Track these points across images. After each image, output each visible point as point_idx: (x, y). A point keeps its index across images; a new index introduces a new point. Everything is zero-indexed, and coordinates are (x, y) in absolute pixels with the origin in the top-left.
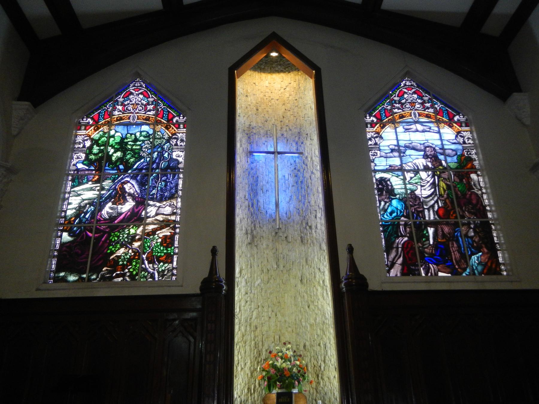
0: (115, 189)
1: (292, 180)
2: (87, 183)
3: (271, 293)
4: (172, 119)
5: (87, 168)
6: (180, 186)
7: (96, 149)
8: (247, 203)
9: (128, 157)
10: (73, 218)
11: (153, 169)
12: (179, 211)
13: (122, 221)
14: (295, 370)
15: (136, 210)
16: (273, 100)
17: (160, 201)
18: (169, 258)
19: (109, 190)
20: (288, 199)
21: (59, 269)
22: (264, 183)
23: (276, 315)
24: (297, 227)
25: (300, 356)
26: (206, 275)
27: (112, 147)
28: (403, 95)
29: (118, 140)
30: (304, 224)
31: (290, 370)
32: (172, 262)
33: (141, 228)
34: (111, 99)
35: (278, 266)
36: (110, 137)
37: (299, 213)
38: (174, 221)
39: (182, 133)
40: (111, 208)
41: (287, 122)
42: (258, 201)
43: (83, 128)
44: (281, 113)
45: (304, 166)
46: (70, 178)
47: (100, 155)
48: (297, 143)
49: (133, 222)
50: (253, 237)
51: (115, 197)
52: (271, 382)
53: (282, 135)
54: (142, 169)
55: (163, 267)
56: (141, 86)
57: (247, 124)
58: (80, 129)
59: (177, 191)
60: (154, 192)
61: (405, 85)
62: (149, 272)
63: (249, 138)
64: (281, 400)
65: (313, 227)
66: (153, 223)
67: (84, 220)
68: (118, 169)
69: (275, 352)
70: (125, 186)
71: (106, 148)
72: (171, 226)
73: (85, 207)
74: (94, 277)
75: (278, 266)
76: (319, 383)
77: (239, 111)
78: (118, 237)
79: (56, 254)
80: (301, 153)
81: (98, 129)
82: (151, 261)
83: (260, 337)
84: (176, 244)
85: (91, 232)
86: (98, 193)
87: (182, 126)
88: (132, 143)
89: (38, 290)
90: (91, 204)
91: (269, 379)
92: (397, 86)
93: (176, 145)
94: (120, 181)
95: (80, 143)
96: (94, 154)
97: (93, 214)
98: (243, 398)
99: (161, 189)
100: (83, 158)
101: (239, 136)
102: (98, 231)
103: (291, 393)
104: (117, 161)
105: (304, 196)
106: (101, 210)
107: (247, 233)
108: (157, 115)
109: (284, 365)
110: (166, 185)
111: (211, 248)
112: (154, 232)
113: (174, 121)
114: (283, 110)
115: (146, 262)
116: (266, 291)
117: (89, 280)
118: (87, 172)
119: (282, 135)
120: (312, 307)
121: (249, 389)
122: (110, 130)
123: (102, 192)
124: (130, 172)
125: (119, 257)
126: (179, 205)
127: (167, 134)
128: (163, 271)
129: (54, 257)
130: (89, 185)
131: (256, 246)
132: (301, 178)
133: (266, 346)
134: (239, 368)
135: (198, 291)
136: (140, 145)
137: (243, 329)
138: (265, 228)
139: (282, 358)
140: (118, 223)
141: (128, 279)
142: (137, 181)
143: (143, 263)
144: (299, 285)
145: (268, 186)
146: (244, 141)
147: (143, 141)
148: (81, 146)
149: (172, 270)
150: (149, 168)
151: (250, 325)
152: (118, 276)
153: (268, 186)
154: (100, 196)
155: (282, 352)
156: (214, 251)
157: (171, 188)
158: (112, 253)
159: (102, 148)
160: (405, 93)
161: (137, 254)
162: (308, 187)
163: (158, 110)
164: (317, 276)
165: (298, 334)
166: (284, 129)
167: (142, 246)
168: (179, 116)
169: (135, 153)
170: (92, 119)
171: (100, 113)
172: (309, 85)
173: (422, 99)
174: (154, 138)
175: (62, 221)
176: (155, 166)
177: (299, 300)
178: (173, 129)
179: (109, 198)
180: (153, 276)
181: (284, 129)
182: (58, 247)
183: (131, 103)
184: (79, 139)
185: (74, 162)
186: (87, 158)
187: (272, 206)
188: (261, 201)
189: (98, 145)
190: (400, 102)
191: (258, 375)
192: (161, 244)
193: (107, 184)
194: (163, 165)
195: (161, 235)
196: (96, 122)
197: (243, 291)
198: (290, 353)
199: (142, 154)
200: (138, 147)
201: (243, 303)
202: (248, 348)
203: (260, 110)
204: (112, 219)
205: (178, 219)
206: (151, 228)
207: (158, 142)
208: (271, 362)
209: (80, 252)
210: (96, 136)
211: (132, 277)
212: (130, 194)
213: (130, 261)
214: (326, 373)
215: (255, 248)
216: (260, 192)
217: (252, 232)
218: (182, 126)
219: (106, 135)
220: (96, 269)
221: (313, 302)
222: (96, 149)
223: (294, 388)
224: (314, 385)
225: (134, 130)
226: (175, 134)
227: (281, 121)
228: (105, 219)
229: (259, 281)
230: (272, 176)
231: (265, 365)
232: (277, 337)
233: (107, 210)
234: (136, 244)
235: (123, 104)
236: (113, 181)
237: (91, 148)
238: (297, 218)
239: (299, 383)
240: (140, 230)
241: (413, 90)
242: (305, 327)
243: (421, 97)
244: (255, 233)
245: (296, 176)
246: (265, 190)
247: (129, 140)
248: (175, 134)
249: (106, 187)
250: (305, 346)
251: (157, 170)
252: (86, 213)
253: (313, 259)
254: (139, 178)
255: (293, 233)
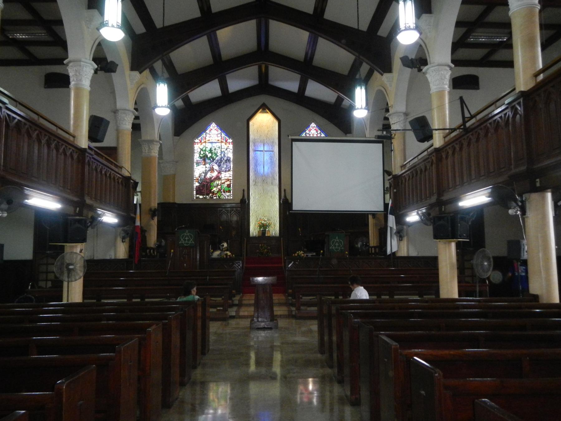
0: (210, 168)
1: (269, 161)
2: (201, 165)
3: (261, 201)
4: (227, 141)
5: (200, 160)
6: (232, 167)
7: (202, 153)
8: (253, 170)
9: (213, 156)
10: (198, 178)
11: (222, 160)
12: (232, 176)
13: (214, 179)
14: (267, 224)
15: (218, 175)
16: (263, 127)
17: (225, 172)
18: (229, 191)
19: (208, 168)
20: (268, 168)
21: (197, 194)
22: (260, 162)
23: (263, 208)
24: (270, 179)
25: (270, 220)
26: (241, 197)
27: (208, 152)
28: (310, 130)
29: (209, 149)
30: (273, 178)
31: (266, 224)
32: (231, 192)
33: (220, 181)
34: (205, 130)
35: (264, 192)
36: (206, 148)
37: (271, 174)
38: (230, 179)
39: (231, 146)
40: (210, 175)
41: (269, 136)
42: (257, 169)
43: (196, 144)
44: (266, 132)
45: (274, 156)
46: (195, 163)
47: (204, 155)
48: (272, 146)
49: (218, 179)
50: (256, 182)
51: (210, 170)
52: (260, 227)
53: (267, 142)
54: (218, 160)
55: (228, 194)
56: (215, 126)
57: (254, 138)
58: (195, 144)
59: (230, 169)
60: (223, 169)
61: (312, 126)
62: (224, 196)
63: (254, 144)
64: (263, 232)
65: (276, 179)
66: (224, 180)
67: (202, 178)
68: (210, 160)
69: (262, 219)
70: (213, 166)
71: (205, 152)
72: (230, 180)
73: (201, 174)
74: (207, 197)
75: (264, 192)
76: (275, 228)
77: (251, 133)
78: (213, 184)
79: (195, 189)
80: (273, 151)
81: (202, 144)
82: (224, 192)
83: (257, 215)
84: (231, 187)
85: (204, 182)
86: (205, 169)
87: (231, 143)
88: (214, 150)
89: (192, 201)
90: (203, 173)
91: (260, 226)
92: (309, 126)
93: (229, 151)
94: (212, 165)
95: (196, 150)
96: (202, 155)
97: (205, 176)
98: (252, 231)
99: (225, 168)
100: (199, 156)
101: (251, 144)
102: (207, 182)
103: (265, 230)
104: (210, 157)
105: (273, 168)
106: (206, 175)
107: (253, 181)
108: (221, 139)
109: (264, 223)
110: (227, 166)
111: (243, 189)
112: (224, 183)
113: (228, 141)
114: (267, 130)
115: (223, 192)
116: (260, 200)
117: (206, 198)
118: (200, 161)
119: (267, 142)
120: (274, 206)
121: (254, 229)
122: (206, 144)
123: (207, 169)
124: (214, 161)
125: (214, 191)
126: (232, 174)
127: (226, 147)
128: (228, 195)
129: (194, 190)
130: (202, 166)
131: (257, 185)
132: (273, 161)
133: (259, 217)
134: (251, 223)
135: (239, 202)
136: (217, 151)
137: (252, 212)
138: (260, 179)
139: (264, 221)
140: (213, 179)
141: (218, 198)
142: (217, 165)
143: (222, 193)
144: (270, 199)
145: (261, 163)
146: (252, 146)
147: (218, 150)
148: (197, 151)
149: (231, 195)
150: (221, 160)
151: (255, 211)
152: (215, 197)
153: (261, 163)
154: (206, 170)
155: (263, 219)
156: (244, 190)
157: (229, 168)
158: (212, 189)
159: (204, 152)
160: (311, 130)
161: (220, 190)
162: (275, 164)
163: (222, 137)
164: (276, 196)
165: (269, 214)
166: (267, 140)
167: (221, 187)
168: (229, 139)
169: (215, 154)
170: (199, 140)
171: (201, 138)
172: (276, 123)
173: (317, 132)
174: (221, 148)
175: (195, 178)
176: (222, 159)
177: (270, 203)
178: (228, 145)
179: (209, 170)
180: (225, 197)
181: (267, 140)
182: (195, 187)
183: (212, 134)
184: (195, 148)
185: (195, 157)
186: (200, 156)
187: (262, 171)
188: (258, 169)
189: (203, 151)
190: (309, 134)
191: (257, 225)
192: (227, 187)
193: (208, 165)
194: (225, 159)
195: (227, 184)
196: (201, 142)
197: (252, 201)
198: (266, 219)
199: (218, 154)
200: (216, 152)
201: (252, 204)
202: (254, 218)
203: (259, 131)
204: (211, 178)
205: (231, 178)
206: (223, 181)
207: (222, 150)
208: (260, 222)
209: (202, 189)
210: (201, 147)
211: (219, 197)
212: (215, 170)
213: (218, 192)
214: (277, 225)
215: (256, 186)
216: (258, 166)
217: (255, 180)
218: (231, 143)
219: (205, 147)
220: (208, 194)
221: (274, 204)
222: (202, 153)
223: (267, 228)
224: (273, 228)
225: (214, 145)
226: (228, 147)
227: (266, 136)
228: (208, 178)
229: (257, 197)
230: (262, 159)
231: (259, 222)
232: (263, 214)
233: (208, 176)
234: (219, 187)
235: (209, 134)
236: (209, 165)
237: (200, 152)
238: (271, 175)
239: (268, 227)
240: (220, 182)
241: (315, 128)
242: (272, 211)
243: (317, 131)
244: (256, 181)
245: (271, 159)
246: (260, 165)
247: (213, 149)
248: (228, 147)
249: (207, 167)
250: (271, 217)
251: (224, 161)
252: (202, 176)
253: (275, 191)
254: (218, 164)
255: (269, 180)
